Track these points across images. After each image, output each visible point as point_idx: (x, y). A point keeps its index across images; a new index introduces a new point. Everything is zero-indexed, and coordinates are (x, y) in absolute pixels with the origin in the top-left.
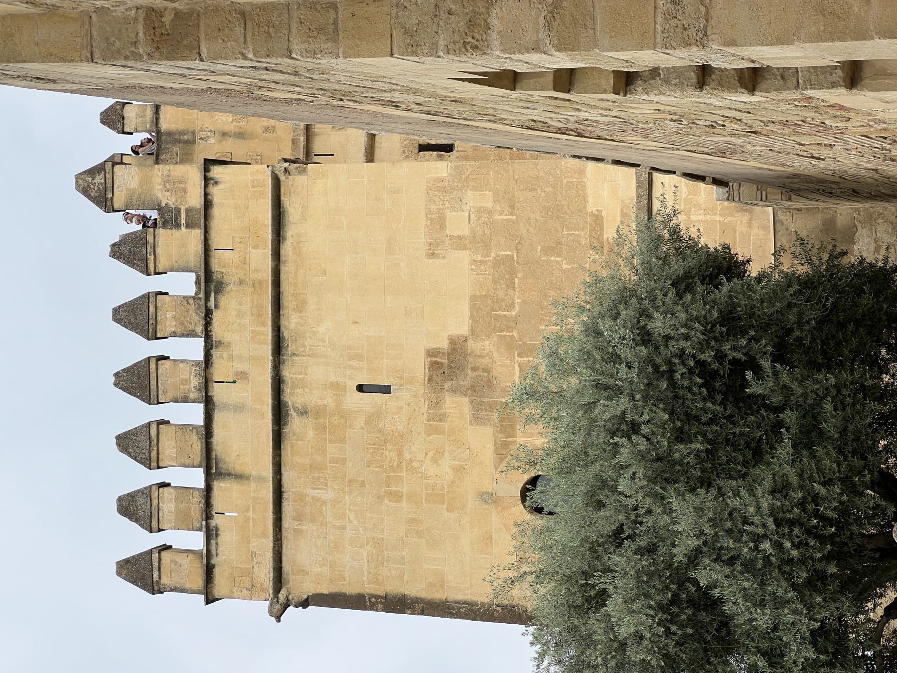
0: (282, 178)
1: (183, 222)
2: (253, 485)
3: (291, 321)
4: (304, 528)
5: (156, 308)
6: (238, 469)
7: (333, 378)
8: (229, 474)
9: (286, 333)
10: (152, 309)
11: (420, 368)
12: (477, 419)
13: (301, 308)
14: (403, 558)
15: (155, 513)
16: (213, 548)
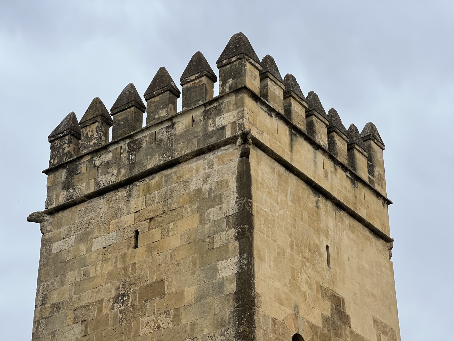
0: (388, 244)
1: (370, 177)
2: (289, 153)
3: (347, 220)
4: (276, 175)
5: (343, 139)
6: (294, 147)
7: (330, 233)
8: (292, 140)
9: (342, 213)
10: (344, 137)
11: (342, 291)
12: (324, 319)
13: (352, 229)
14: (269, 237)
15: (275, 80)
16: (264, 107)
